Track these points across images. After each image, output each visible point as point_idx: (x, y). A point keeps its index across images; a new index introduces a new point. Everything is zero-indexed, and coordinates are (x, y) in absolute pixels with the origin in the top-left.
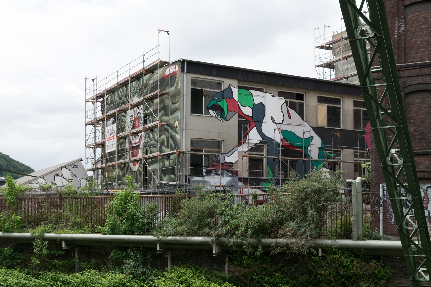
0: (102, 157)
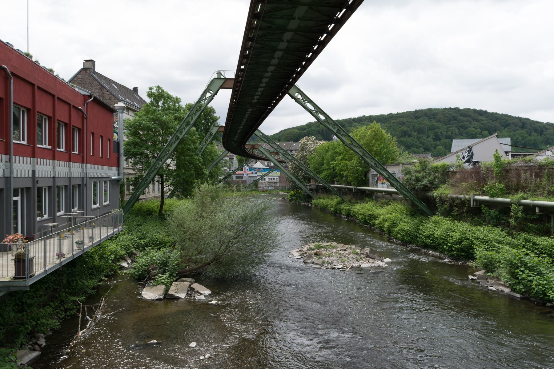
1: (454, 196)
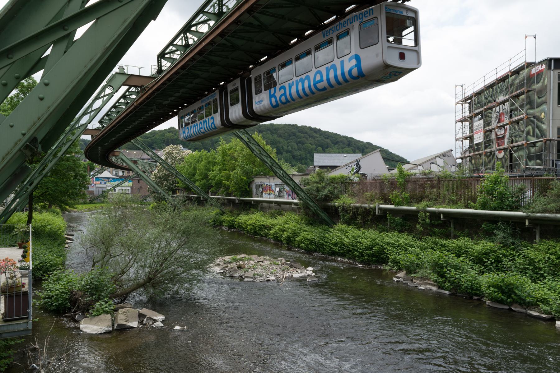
0: (469, 148)
1: (358, 205)
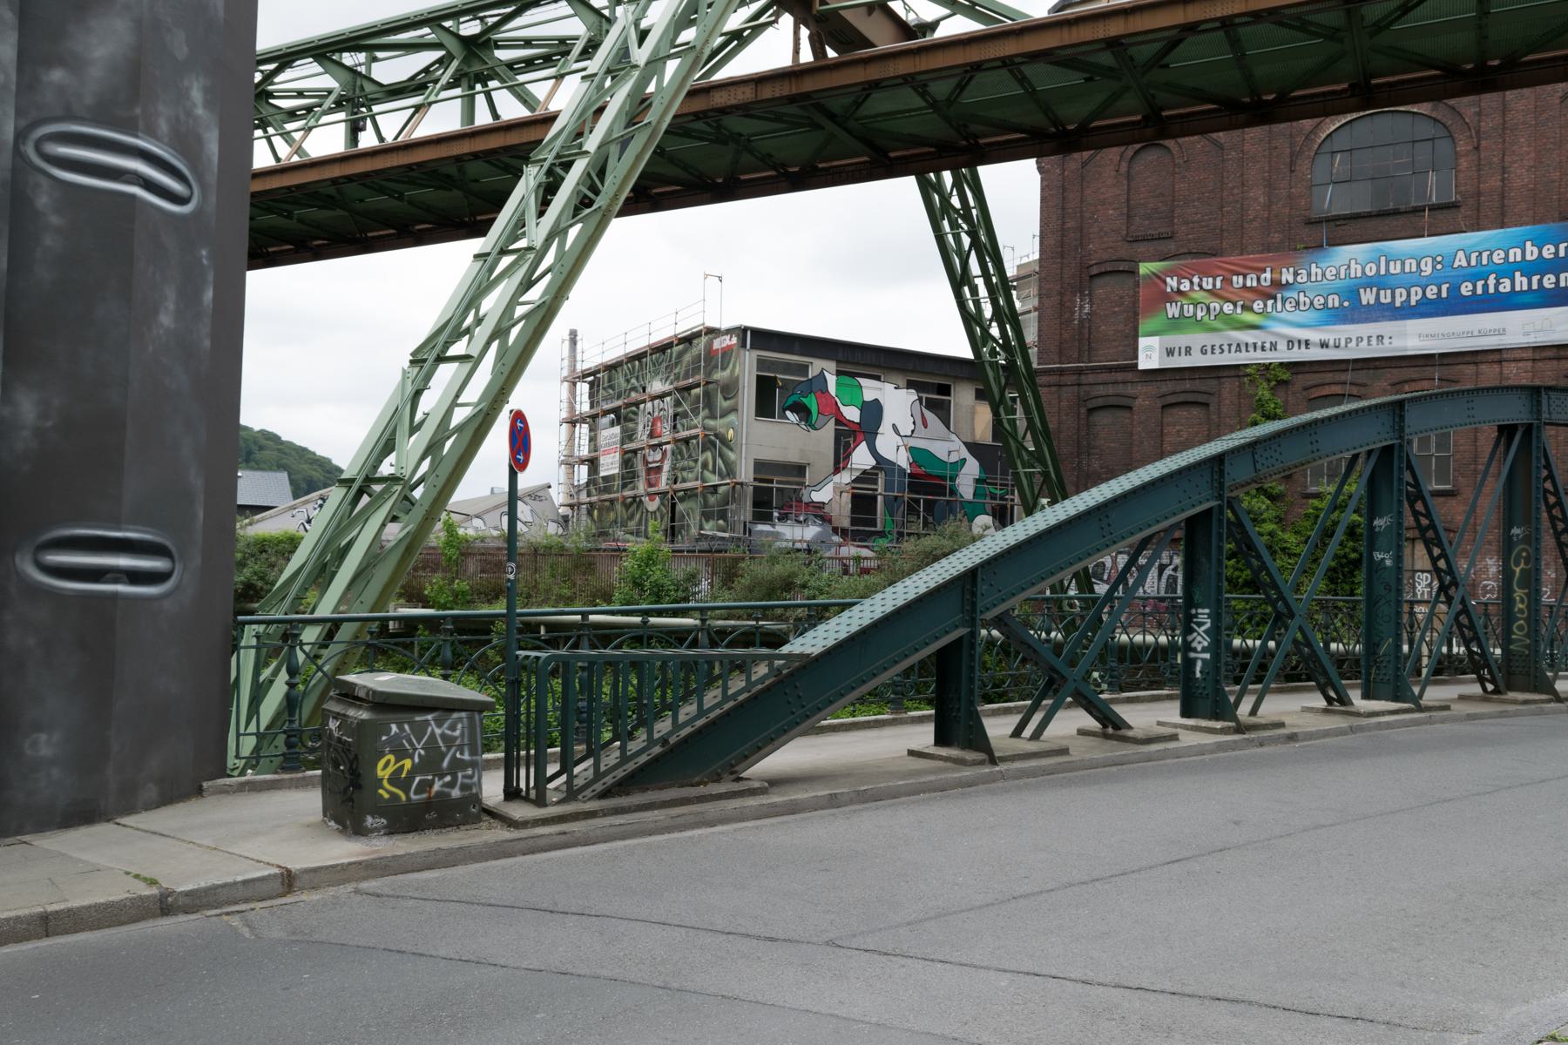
0: (588, 484)
